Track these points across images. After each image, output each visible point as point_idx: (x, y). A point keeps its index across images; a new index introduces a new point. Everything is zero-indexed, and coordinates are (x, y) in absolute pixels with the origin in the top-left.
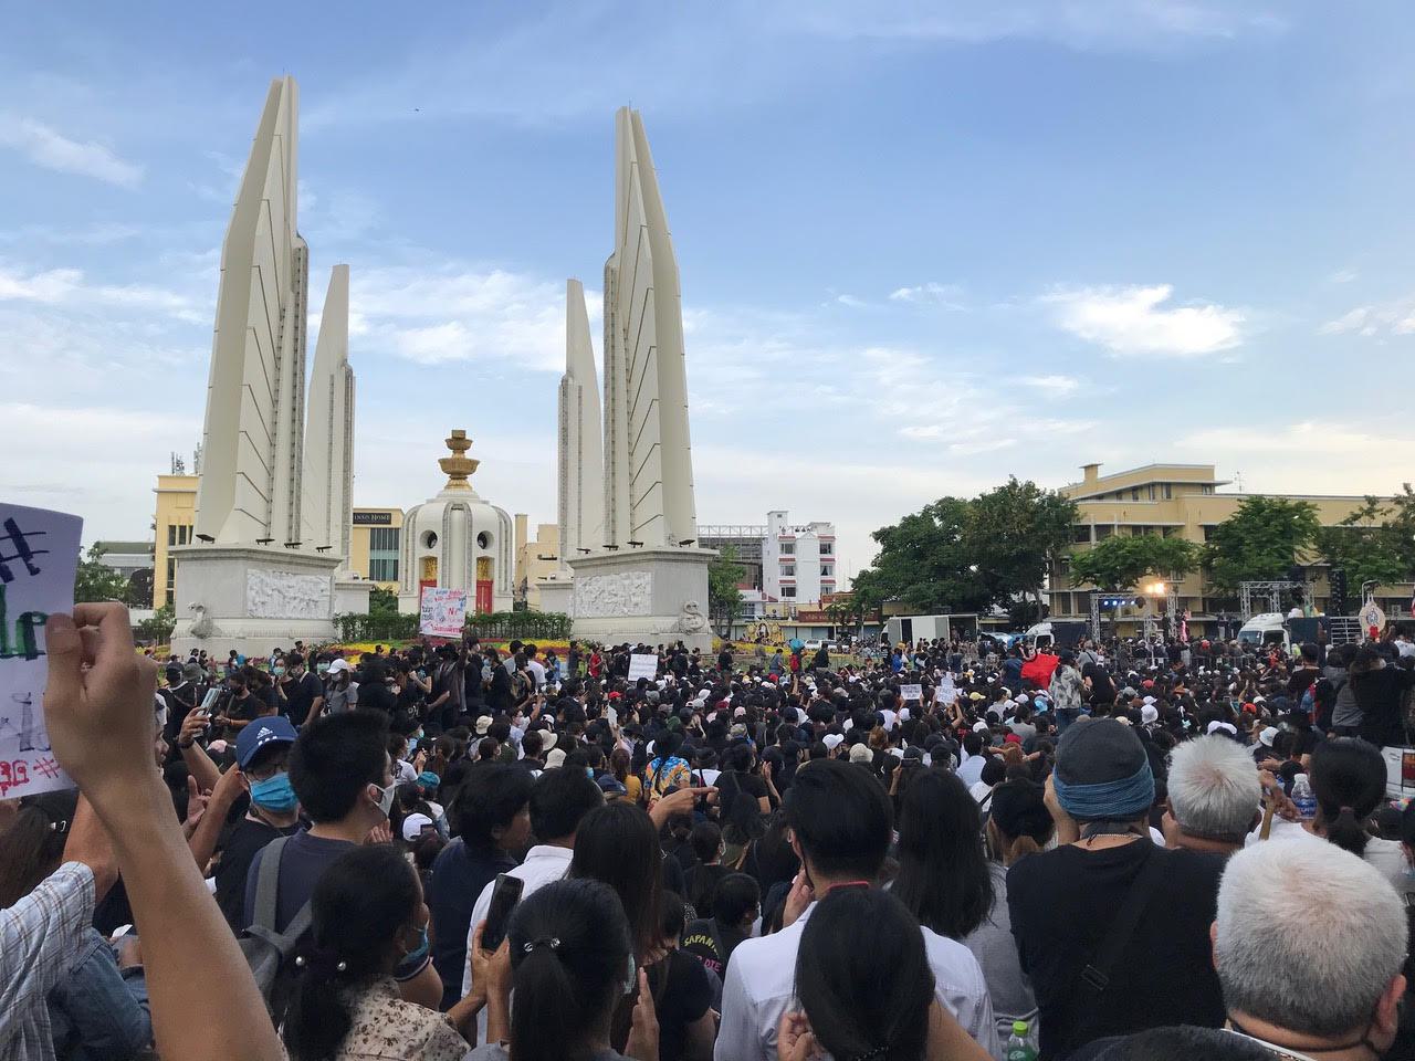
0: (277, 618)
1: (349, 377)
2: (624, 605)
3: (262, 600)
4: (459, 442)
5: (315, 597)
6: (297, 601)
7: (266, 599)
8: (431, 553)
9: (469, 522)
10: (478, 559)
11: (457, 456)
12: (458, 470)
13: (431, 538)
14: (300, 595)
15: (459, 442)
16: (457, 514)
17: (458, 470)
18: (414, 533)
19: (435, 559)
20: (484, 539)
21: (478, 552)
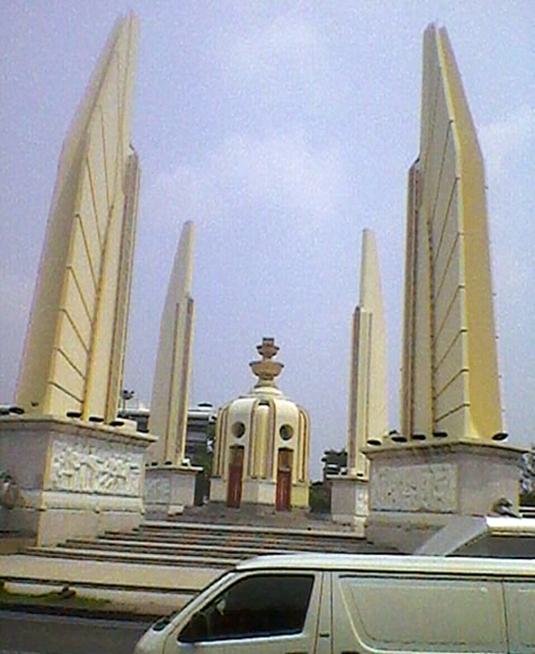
0: (83, 492)
1: (191, 301)
2: (425, 499)
3: (68, 472)
4: (268, 348)
5: (123, 474)
6: (106, 476)
7: (71, 472)
8: (239, 441)
9: (273, 414)
10: (280, 450)
11: (267, 360)
12: (266, 372)
13: (240, 430)
14: (107, 470)
15: (268, 348)
16: (266, 408)
17: (266, 372)
18: (226, 423)
19: (242, 447)
20: (286, 432)
21: (280, 443)
